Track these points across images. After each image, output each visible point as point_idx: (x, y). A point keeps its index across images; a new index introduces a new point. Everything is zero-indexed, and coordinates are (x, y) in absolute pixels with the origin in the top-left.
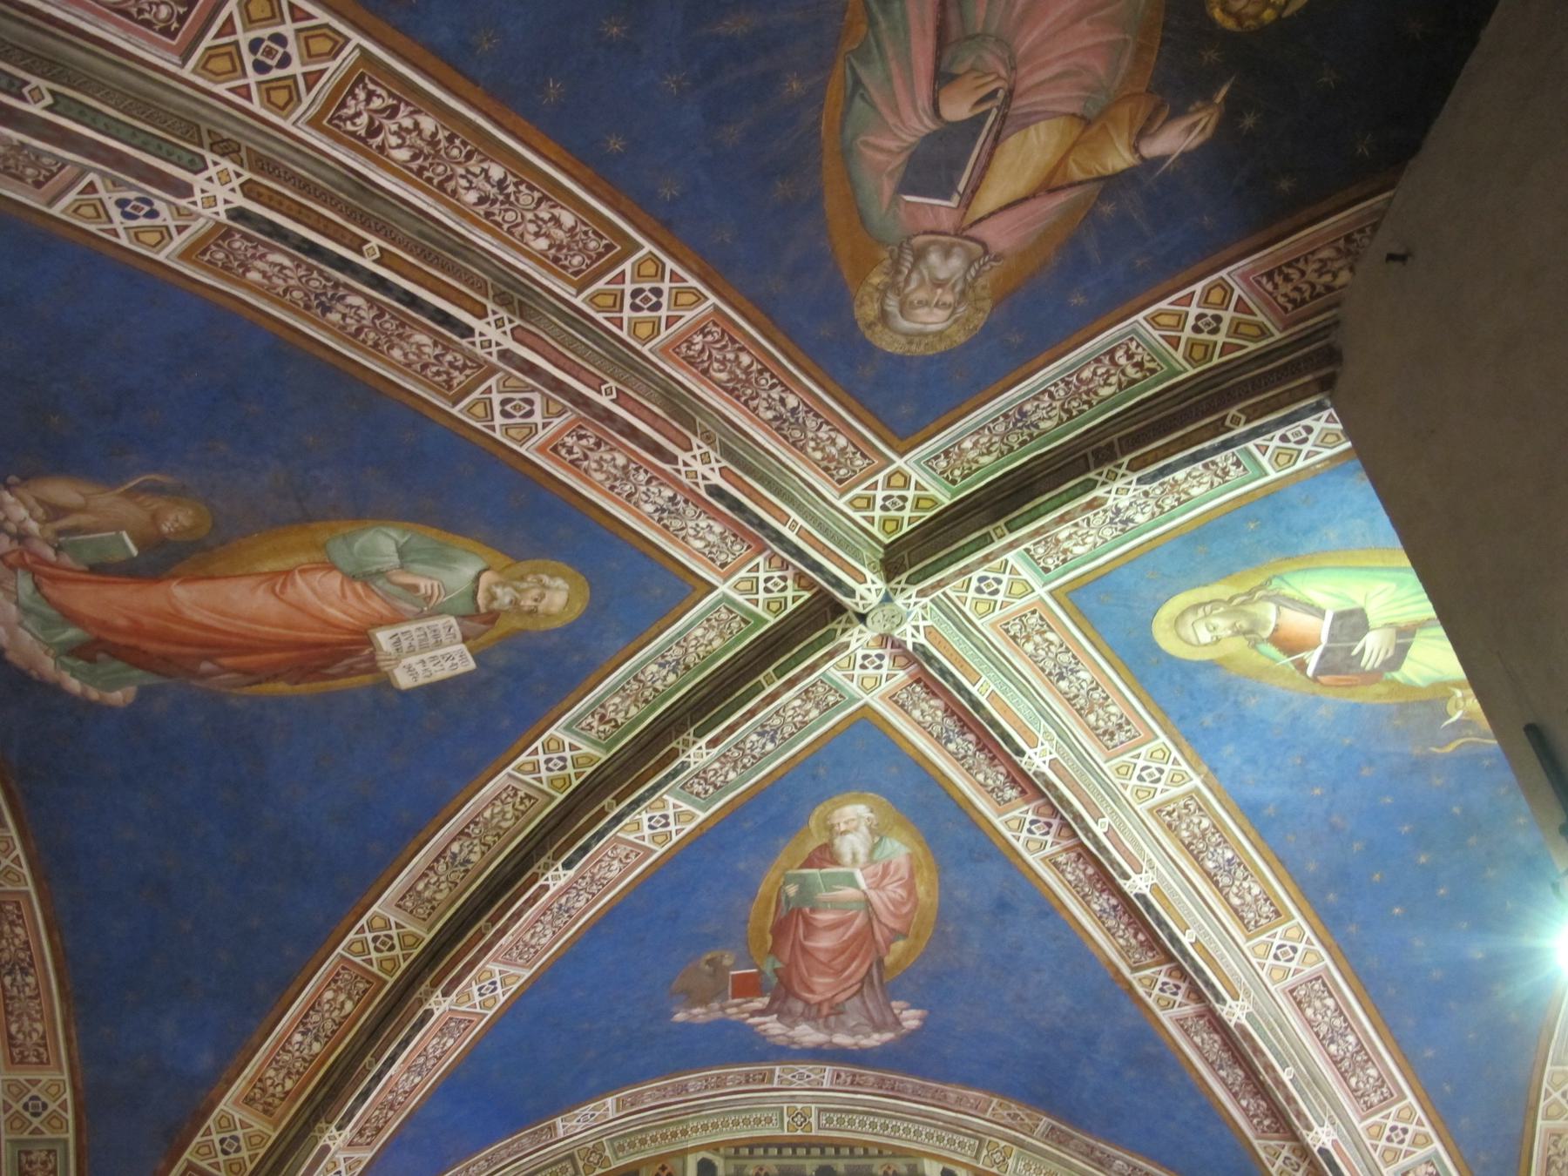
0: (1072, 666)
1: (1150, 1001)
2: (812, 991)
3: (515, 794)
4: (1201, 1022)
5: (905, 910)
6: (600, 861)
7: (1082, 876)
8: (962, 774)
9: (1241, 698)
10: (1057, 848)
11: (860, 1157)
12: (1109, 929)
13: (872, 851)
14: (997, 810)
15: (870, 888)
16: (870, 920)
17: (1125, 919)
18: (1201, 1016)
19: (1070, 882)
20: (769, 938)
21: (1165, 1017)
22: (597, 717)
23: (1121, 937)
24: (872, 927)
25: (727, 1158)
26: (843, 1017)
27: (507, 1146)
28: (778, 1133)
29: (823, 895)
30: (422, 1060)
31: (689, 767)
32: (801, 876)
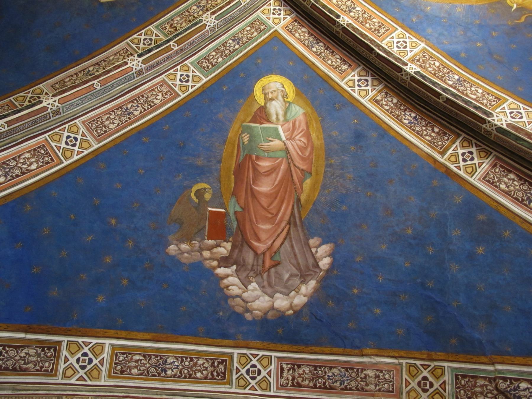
0: (353, 6)
1: (461, 173)
2: (258, 240)
3: (126, 52)
4: (497, 170)
5: (307, 153)
6: (153, 90)
7: (392, 105)
8: (321, 61)
9: (423, 8)
10: (375, 92)
12: (418, 133)
13: (286, 113)
14: (341, 77)
15: (287, 139)
16: (289, 164)
17: (423, 123)
18: (495, 166)
19: (387, 110)
20: (233, 176)
21: (474, 180)
22: (169, 24)
23: (426, 135)
24: (290, 169)
26: (279, 268)
27: (18, 346)
29: (264, 145)
30: (13, 164)
31: (202, 22)
32: (250, 127)
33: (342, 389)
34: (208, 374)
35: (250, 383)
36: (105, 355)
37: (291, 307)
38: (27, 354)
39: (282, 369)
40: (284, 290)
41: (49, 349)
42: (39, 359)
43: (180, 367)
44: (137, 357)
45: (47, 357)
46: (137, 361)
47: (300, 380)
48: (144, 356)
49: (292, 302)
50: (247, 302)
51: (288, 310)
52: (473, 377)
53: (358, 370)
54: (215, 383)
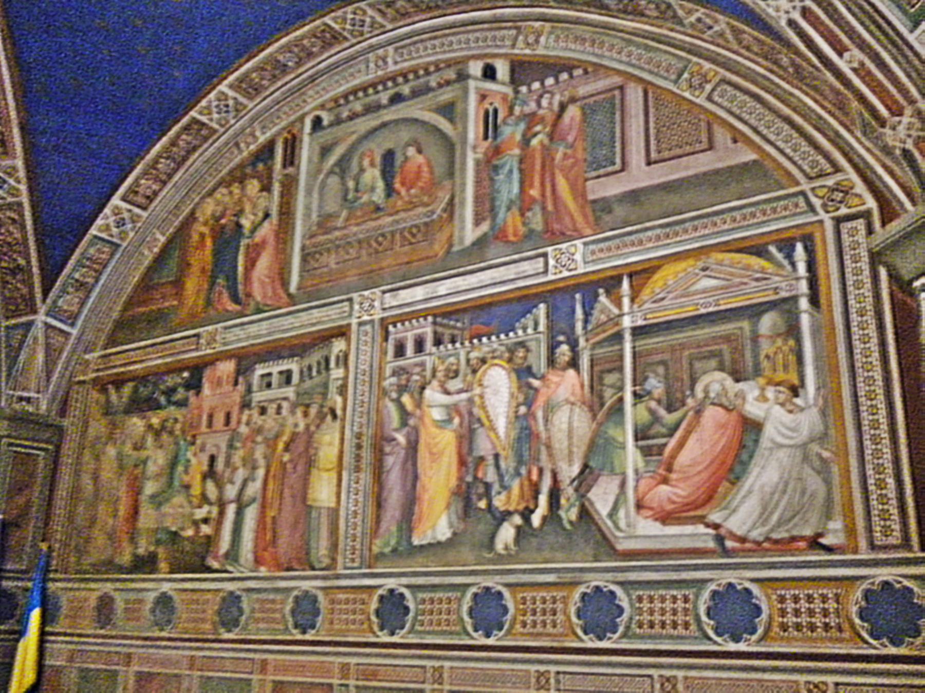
25: (330, 110)
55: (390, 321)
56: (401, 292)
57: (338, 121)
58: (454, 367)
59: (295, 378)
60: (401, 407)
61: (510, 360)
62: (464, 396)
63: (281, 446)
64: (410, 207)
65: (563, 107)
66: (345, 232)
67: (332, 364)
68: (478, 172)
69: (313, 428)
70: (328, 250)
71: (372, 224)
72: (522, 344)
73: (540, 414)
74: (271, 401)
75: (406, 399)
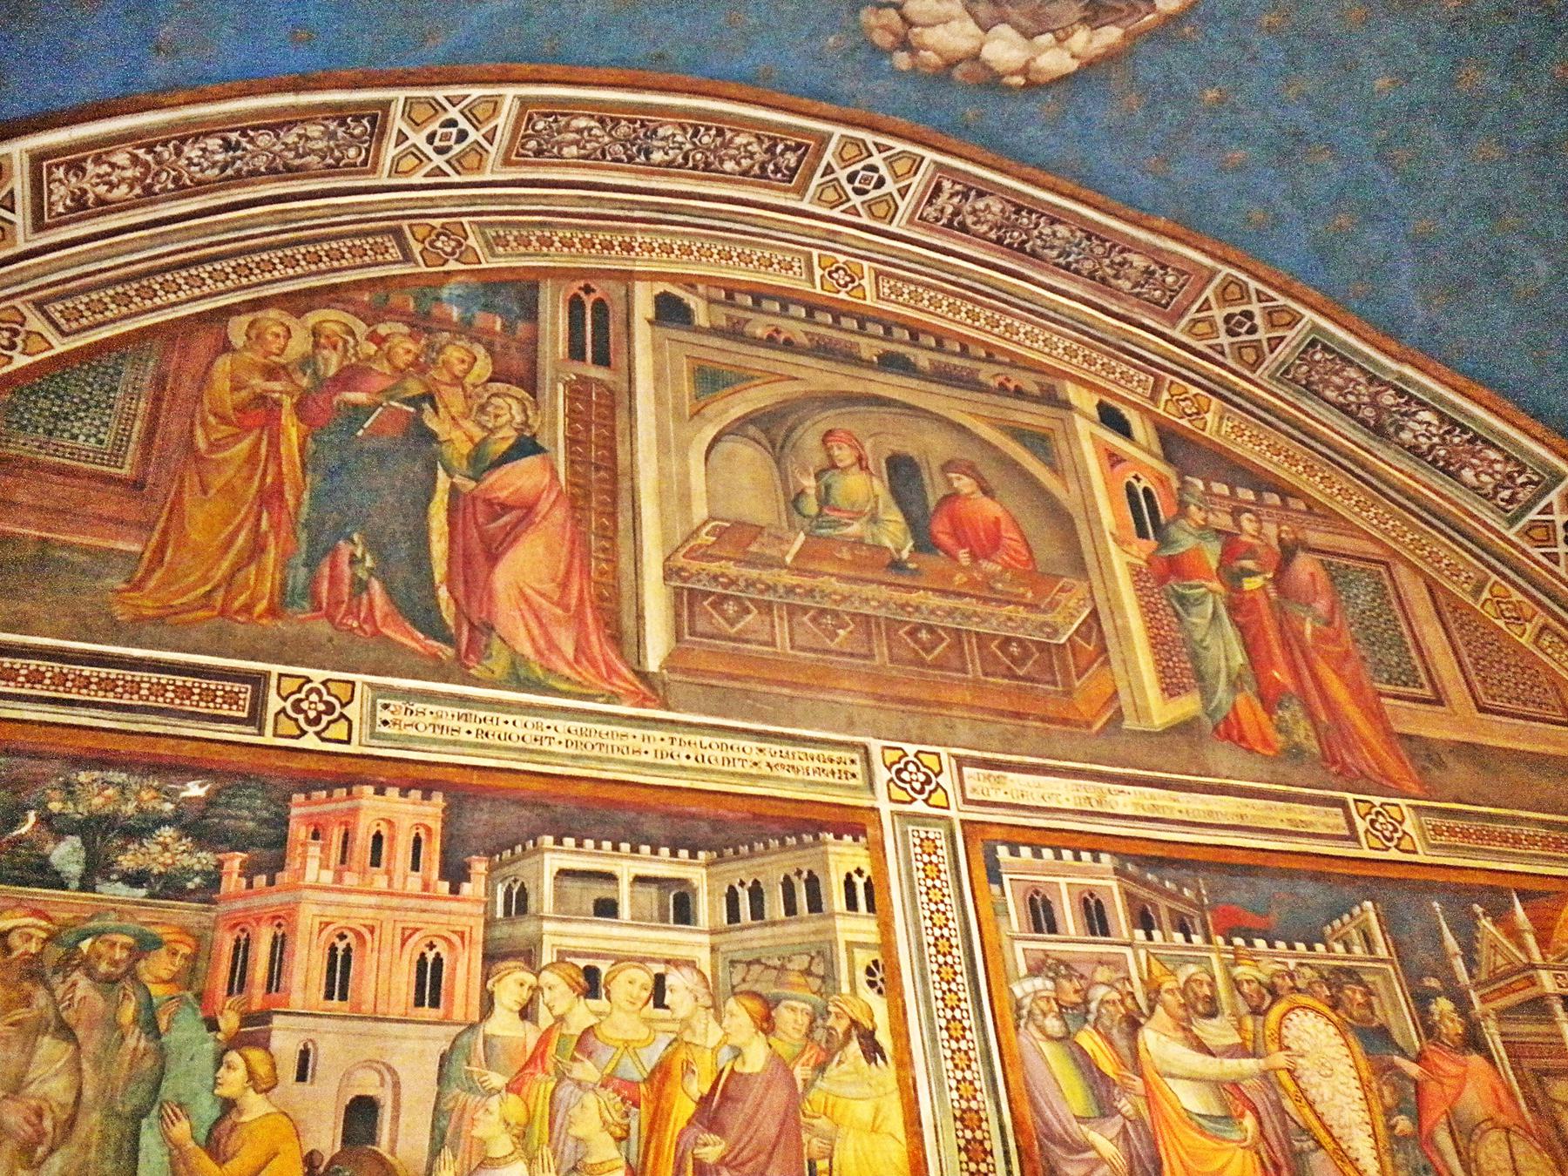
11: (954, 354)
25: (711, 301)
27: (278, 123)
28: (807, 287)
33: (1057, 265)
34: (752, 166)
35: (848, 200)
36: (500, 121)
37: (1025, 70)
38: (300, 136)
39: (938, 189)
40: (1024, 22)
41: (357, 119)
42: (332, 143)
43: (688, 146)
44: (582, 123)
45: (352, 135)
46: (579, 131)
47: (970, 220)
48: (601, 121)
49: (1034, 59)
50: (912, 25)
51: (1012, 74)
52: (1343, 359)
53: (1114, 246)
54: (766, 186)
55: (998, 833)
56: (1010, 775)
57: (735, 333)
58: (1206, 990)
59: (708, 908)
60: (1085, 1064)
61: (1335, 1005)
62: (1249, 1065)
63: (683, 1108)
64: (986, 594)
65: (1288, 553)
66: (808, 582)
67: (836, 898)
68: (1139, 590)
69: (800, 1073)
70: (766, 608)
71: (884, 592)
72: (1351, 973)
73: (1443, 1139)
74: (619, 959)
75: (1088, 1040)
